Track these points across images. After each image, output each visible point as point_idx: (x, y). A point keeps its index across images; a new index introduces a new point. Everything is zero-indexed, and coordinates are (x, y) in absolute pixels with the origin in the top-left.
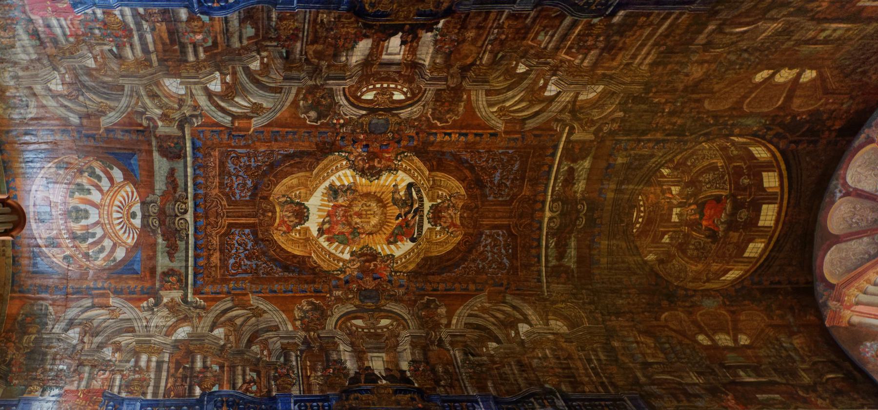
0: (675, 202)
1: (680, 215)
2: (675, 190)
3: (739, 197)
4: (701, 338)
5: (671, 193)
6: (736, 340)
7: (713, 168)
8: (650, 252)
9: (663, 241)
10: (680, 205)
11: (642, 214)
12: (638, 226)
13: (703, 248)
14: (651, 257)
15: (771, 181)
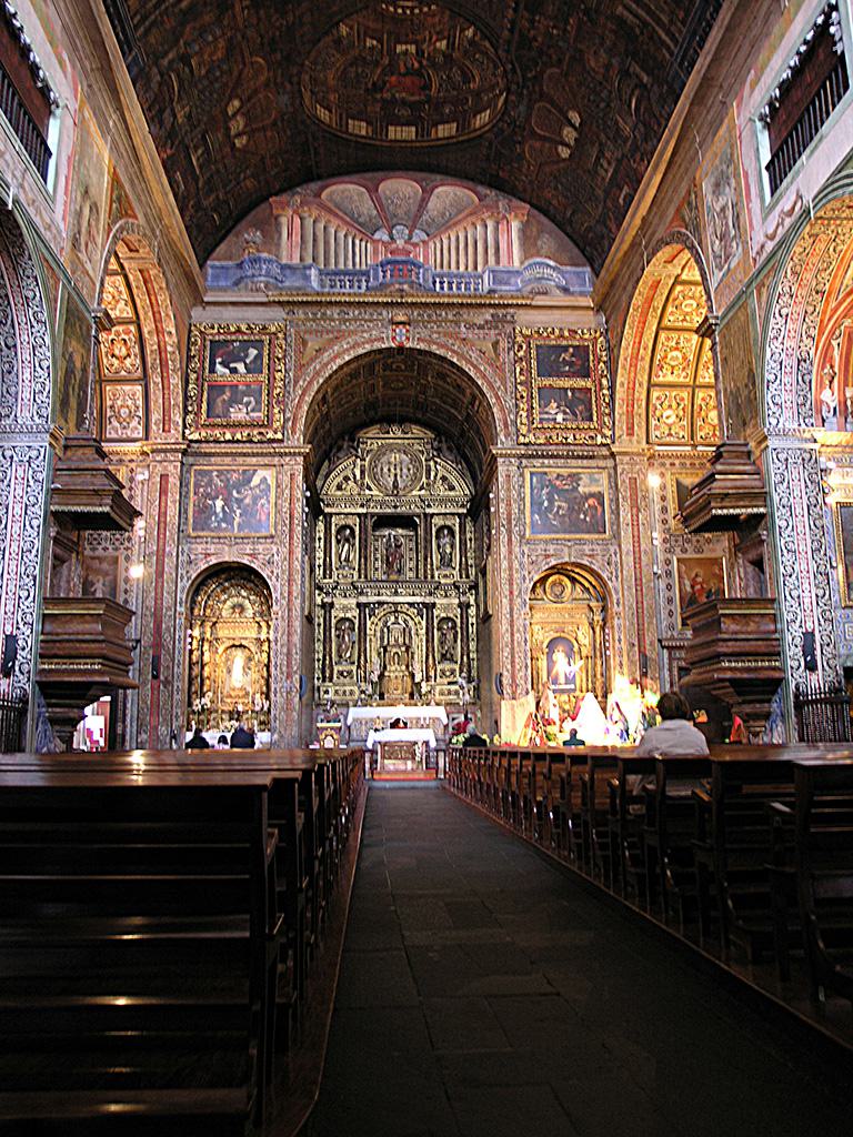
0: (425, 46)
1: (406, 53)
2: (442, 45)
3: (427, 107)
4: (236, 103)
5: (437, 40)
6: (239, 135)
7: (467, 78)
8: (351, 28)
9: (368, 40)
10: (420, 52)
11: (408, 12)
12: (392, 9)
13: (358, 81)
14: (344, 30)
15: (443, 131)
